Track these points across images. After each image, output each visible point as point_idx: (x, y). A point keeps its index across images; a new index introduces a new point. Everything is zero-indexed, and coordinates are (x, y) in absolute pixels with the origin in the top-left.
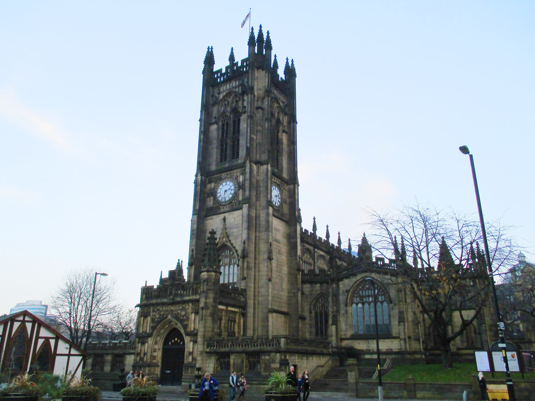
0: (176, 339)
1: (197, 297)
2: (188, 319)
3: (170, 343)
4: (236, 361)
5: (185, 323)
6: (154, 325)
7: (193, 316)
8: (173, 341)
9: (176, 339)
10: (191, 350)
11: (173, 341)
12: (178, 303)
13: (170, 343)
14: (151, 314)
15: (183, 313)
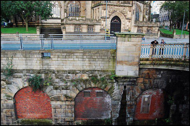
0: (116, 20)
1: (131, 5)
2: (127, 13)
3: (113, 21)
4: (144, 29)
5: (125, 15)
6: (110, 14)
7: (129, 12)
8: (114, 21)
9: (116, 20)
10: (128, 25)
11: (114, 21)
12: (122, 6)
13: (113, 21)
14: (108, 9)
15: (124, 11)
